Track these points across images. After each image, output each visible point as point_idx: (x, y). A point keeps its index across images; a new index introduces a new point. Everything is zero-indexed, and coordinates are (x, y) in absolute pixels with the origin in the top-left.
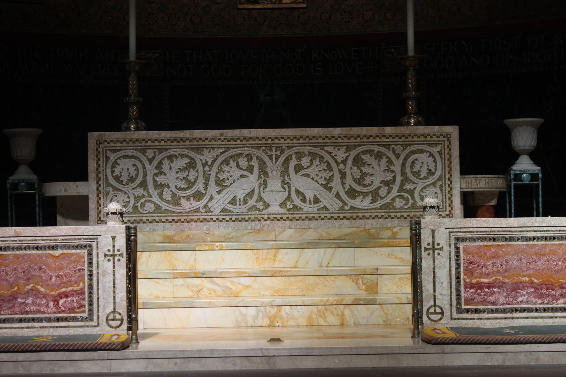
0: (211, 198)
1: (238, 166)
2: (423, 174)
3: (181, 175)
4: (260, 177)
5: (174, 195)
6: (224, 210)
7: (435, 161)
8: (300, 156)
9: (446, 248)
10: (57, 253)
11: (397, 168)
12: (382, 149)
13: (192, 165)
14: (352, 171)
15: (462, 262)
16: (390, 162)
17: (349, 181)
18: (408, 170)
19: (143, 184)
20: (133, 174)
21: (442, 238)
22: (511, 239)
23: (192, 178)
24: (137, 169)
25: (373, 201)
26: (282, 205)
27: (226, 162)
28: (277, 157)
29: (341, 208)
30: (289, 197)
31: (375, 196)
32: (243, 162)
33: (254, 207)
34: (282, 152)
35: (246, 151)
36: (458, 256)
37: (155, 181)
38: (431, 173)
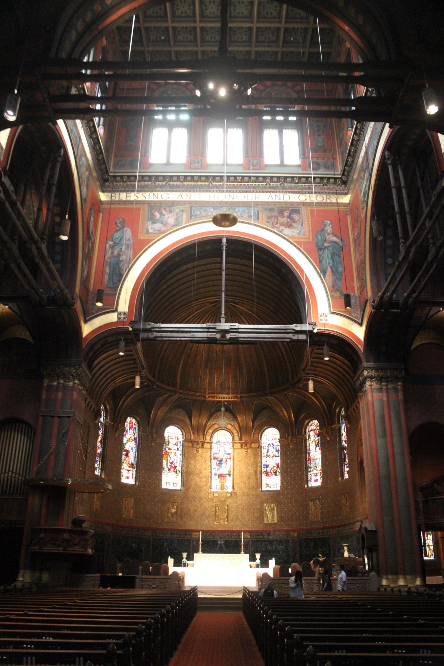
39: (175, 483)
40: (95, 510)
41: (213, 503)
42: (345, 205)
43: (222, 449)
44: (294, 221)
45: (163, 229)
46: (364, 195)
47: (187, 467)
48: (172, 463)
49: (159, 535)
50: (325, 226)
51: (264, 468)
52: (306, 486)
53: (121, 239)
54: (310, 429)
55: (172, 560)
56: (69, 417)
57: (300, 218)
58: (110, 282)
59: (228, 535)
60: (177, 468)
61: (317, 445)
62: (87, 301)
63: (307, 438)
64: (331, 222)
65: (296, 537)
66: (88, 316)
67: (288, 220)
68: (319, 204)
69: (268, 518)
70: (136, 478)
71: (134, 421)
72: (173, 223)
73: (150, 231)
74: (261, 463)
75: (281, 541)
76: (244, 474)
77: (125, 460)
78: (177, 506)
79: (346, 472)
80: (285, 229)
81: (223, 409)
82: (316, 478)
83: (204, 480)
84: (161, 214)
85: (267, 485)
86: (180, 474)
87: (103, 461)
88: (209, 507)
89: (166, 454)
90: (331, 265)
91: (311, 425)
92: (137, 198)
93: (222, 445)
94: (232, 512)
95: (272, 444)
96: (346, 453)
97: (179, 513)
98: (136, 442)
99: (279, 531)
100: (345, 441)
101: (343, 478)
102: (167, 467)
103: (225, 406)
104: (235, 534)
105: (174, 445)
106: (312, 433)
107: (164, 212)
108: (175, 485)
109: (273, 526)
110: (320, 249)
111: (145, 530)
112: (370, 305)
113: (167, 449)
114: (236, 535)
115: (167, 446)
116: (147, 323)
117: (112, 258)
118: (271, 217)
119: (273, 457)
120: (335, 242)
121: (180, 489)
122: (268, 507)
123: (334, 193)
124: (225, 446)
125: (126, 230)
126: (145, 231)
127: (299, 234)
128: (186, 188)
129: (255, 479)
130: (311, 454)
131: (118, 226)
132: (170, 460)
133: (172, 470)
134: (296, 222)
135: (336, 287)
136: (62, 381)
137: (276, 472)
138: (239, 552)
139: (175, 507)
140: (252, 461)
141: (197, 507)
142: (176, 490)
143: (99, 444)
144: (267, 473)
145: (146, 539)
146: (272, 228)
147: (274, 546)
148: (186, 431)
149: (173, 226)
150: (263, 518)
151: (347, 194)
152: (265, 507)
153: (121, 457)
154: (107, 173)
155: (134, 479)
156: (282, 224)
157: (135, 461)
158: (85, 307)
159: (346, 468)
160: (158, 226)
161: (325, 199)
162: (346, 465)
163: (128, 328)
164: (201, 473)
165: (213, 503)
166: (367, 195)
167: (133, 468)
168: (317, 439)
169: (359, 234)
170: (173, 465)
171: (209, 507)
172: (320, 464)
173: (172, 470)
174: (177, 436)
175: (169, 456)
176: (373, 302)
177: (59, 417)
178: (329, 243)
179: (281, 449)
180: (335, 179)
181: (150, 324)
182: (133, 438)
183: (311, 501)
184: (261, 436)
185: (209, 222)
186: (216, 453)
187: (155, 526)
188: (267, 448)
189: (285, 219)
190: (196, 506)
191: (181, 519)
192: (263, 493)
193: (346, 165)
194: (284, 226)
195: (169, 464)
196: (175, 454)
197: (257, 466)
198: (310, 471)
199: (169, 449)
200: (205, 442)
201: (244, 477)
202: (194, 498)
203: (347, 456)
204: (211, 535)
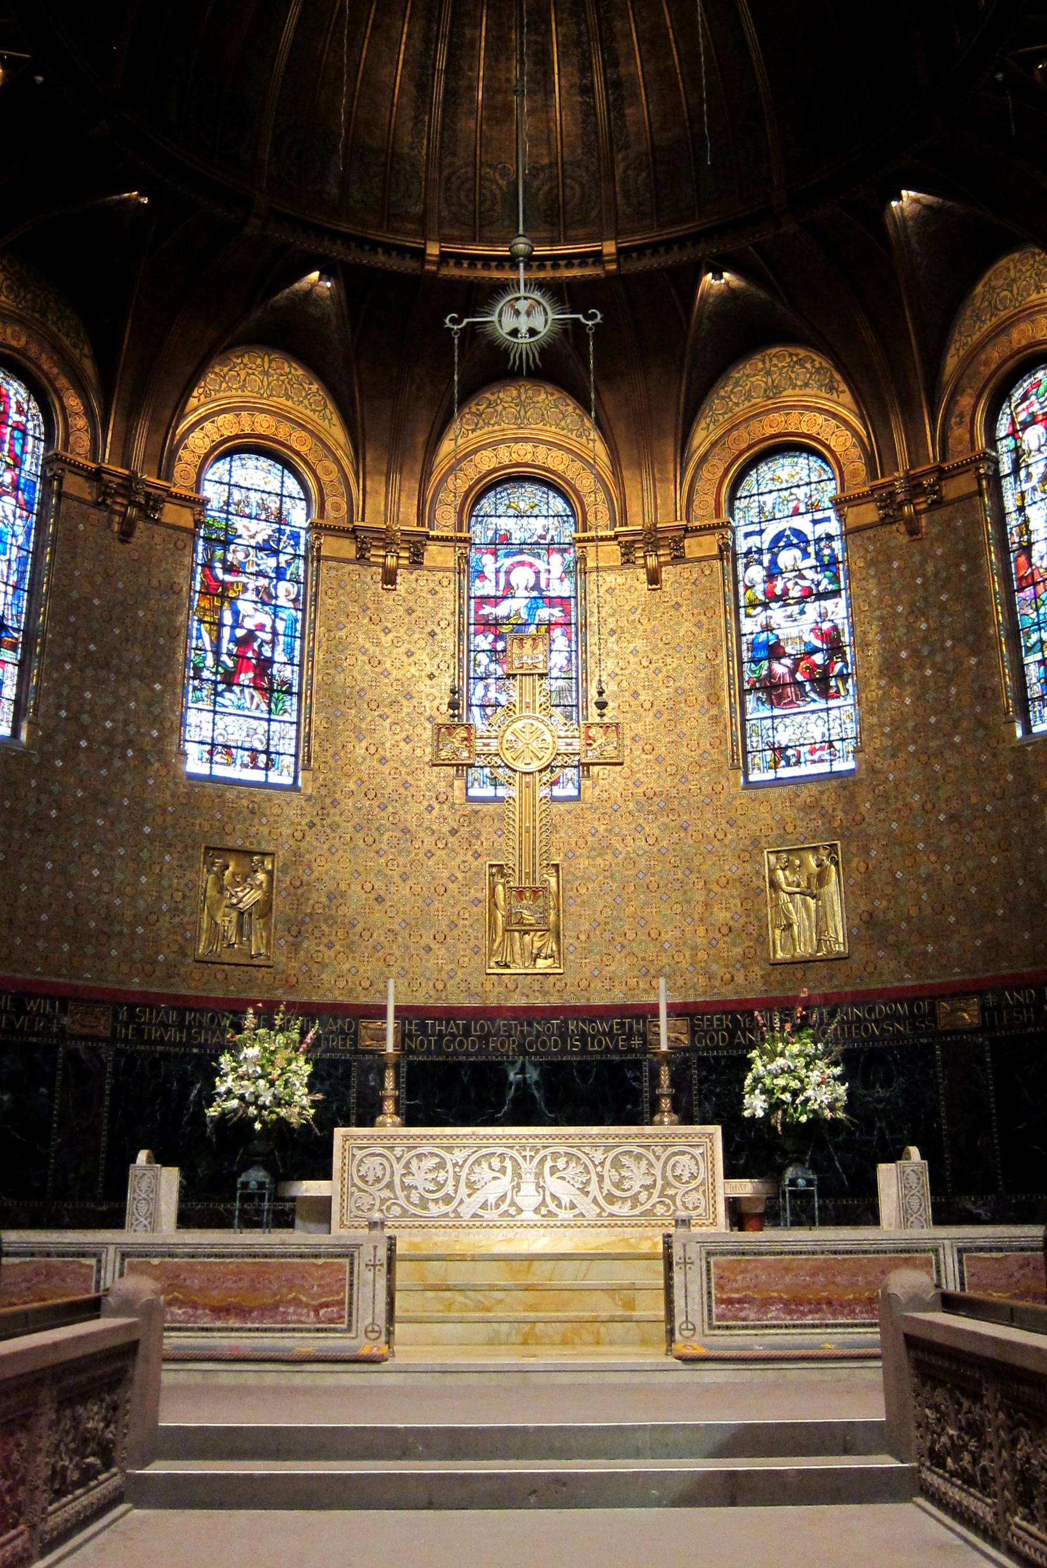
0: (462, 1202)
1: (490, 1167)
2: (685, 1178)
3: (430, 1176)
4: (513, 1180)
5: (422, 1197)
6: (475, 1215)
7: (697, 1164)
8: (555, 1156)
9: (697, 1262)
10: (320, 1261)
11: (657, 1171)
12: (641, 1150)
13: (441, 1165)
14: (610, 1174)
15: (712, 1276)
16: (651, 1165)
17: (607, 1185)
18: (669, 1174)
19: (390, 1186)
20: (380, 1174)
21: (694, 1252)
22: (761, 1254)
23: (441, 1179)
24: (384, 1169)
25: (633, 1208)
26: (537, 1210)
27: (477, 1162)
28: (532, 1157)
29: (599, 1215)
30: (543, 1203)
31: (635, 1200)
32: (496, 1163)
33: (506, 1213)
34: (537, 1151)
35: (499, 1151)
36: (708, 1270)
37: (402, 1182)
38: (693, 1177)
39: (261, 748)
41: (477, 855)
43: (522, 577)
52: (1019, 733)
54: (1022, 417)
55: (170, 1178)
63: (1006, 467)
69: (789, 926)
70: (17, 702)
74: (740, 635)
78: (270, 874)
85: (780, 751)
88: (453, 878)
89: (207, 591)
91: (1025, 397)
95: (798, 533)
97: (277, 902)
98: (27, 506)
102: (218, 662)
104: (601, 1026)
105: (259, 548)
108: (262, 759)
111: (64, 1002)
113: (218, 565)
114: (610, 1034)
115: (219, 553)
119: (801, 600)
121: (289, 781)
124: (541, 565)
132: (236, 625)
133: (245, 678)
137: (825, 679)
139: (261, 877)
142: (266, 785)
148: (324, 478)
152: (772, 871)
164: (409, 696)
165: (477, 855)
171: (453, 878)
173: (245, 678)
174: (273, 503)
175: (232, 601)
179: (845, 549)
184: (733, 498)
188: (766, 558)
191: (296, 947)
192: (752, 793)
195: (226, 645)
199: (230, 569)
200: (428, 537)
201: (649, 718)
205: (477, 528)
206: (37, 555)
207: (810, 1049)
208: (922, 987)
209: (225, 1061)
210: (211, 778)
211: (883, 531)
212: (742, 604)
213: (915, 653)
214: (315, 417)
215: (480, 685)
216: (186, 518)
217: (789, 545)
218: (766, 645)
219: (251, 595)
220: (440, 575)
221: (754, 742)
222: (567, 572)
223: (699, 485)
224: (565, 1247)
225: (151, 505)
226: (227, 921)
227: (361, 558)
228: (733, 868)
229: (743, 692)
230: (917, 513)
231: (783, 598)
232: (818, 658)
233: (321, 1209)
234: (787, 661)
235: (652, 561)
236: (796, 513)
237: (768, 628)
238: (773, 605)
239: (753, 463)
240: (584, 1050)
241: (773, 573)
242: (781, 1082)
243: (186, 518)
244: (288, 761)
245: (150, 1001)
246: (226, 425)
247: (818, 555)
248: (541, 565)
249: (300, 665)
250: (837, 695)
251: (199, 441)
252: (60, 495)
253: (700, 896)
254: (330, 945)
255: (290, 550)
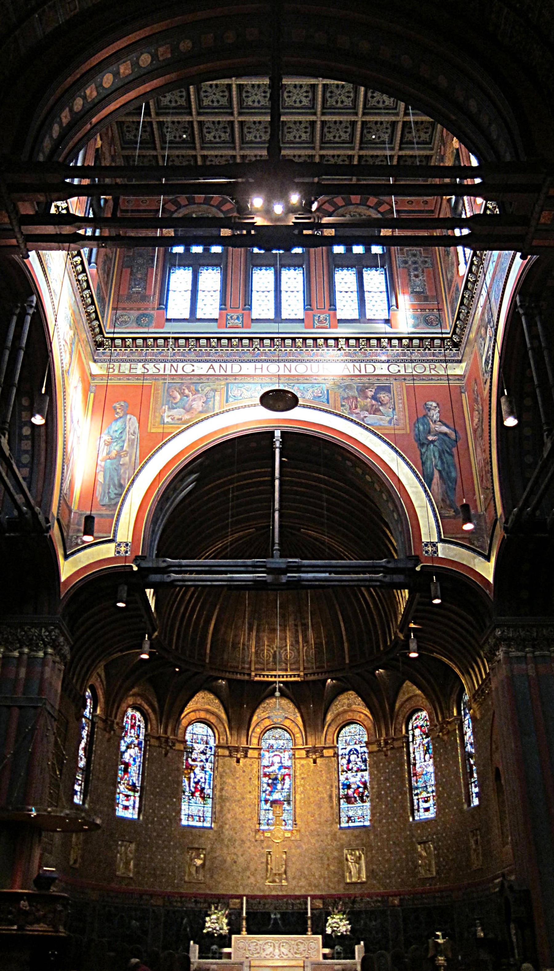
13: (257, 945)
14: (296, 947)
40: (72, 862)
41: (263, 848)
42: (459, 377)
43: (277, 759)
44: (382, 405)
45: (187, 417)
46: (487, 362)
47: (222, 789)
48: (197, 783)
49: (175, 904)
50: (429, 410)
51: (343, 789)
52: (411, 819)
53: (121, 433)
54: (415, 725)
56: (35, 708)
57: (391, 399)
58: (104, 496)
59: (287, 903)
60: (205, 791)
61: (426, 751)
62: (68, 526)
63: (411, 739)
64: (438, 404)
65: (398, 906)
66: (71, 547)
67: (374, 402)
68: (420, 377)
69: (350, 872)
71: (138, 715)
72: (200, 409)
73: (166, 420)
74: (339, 781)
75: (372, 912)
76: (312, 800)
77: (122, 779)
78: (205, 855)
79: (474, 795)
80: (369, 415)
81: (277, 694)
82: (426, 805)
83: (249, 810)
84: (182, 394)
85: (349, 818)
86: (210, 801)
87: (86, 781)
89: (187, 768)
90: (439, 468)
91: (416, 719)
92: (146, 371)
93: (276, 753)
94: (293, 863)
95: (356, 750)
96: (472, 762)
98: (140, 749)
99: (369, 895)
100: (471, 744)
101: (469, 805)
102: (190, 790)
103: (280, 689)
104: (298, 901)
106: (417, 732)
107: (187, 391)
108: (202, 818)
109: (359, 886)
110: (422, 445)
112: (501, 527)
113: (190, 760)
114: (300, 904)
116: (161, 559)
117: (108, 461)
118: (348, 398)
119: (356, 771)
120: (446, 434)
122: (351, 854)
123: (441, 361)
124: (282, 755)
125: (130, 419)
126: (158, 420)
127: (390, 422)
128: (219, 356)
129: (329, 809)
130: (418, 766)
131: (117, 413)
133: (197, 794)
134: (385, 404)
135: (448, 502)
136: (26, 650)
138: (304, 932)
139: (202, 856)
140: (324, 778)
141: (238, 856)
142: (203, 827)
143: (81, 752)
144: (349, 799)
145: (154, 911)
146: (349, 414)
147: (362, 922)
148: (220, 730)
149: (201, 412)
150: (343, 871)
151: (460, 361)
153: (116, 775)
154: (101, 332)
155: (137, 810)
156: (364, 409)
157: (138, 780)
158: (65, 534)
159: (473, 788)
160: (177, 413)
161: (428, 369)
162: (474, 782)
163: (131, 567)
164: (243, 798)
165: (263, 848)
166: (490, 362)
167: (135, 791)
168: (426, 741)
169: (481, 421)
170: (198, 787)
171: (256, 855)
172: (433, 783)
173: (197, 794)
174: (205, 738)
175: (193, 770)
176: (506, 522)
177: (20, 707)
178: (435, 435)
180: (442, 339)
181: (164, 561)
182: (136, 742)
183: (420, 843)
184: (338, 737)
185: (255, 405)
186: (268, 767)
187: (169, 889)
188: (347, 757)
189: (369, 400)
190: (235, 854)
191: (212, 877)
192: (341, 831)
193: (458, 318)
194: (367, 411)
195: (192, 784)
196: (203, 768)
197: (332, 786)
198: (417, 794)
199: (194, 760)
200: (249, 748)
201: (312, 805)
202: (232, 840)
203: (474, 768)
204: (260, 903)
205: (263, 744)
206: (144, 763)
207: (342, 917)
208: (385, 893)
209: (207, 919)
210: (189, 826)
211: (379, 754)
212: (340, 770)
213: (386, 792)
214: (216, 710)
215: (264, 794)
216: (182, 747)
217: (354, 754)
218: (346, 785)
219: (198, 768)
220: (253, 760)
221: (342, 814)
222: (290, 758)
223: (328, 733)
224: (285, 964)
225: (174, 745)
226: (193, 870)
227: (230, 756)
228: (336, 854)
229: (339, 799)
230: (387, 750)
231: (350, 770)
232: (361, 790)
233: (229, 955)
234: (352, 790)
235: (314, 757)
236: (356, 744)
237: (347, 779)
238: (349, 772)
239: (344, 726)
240: (293, 909)
241: (349, 761)
242: (334, 925)
243: (182, 747)
244: (209, 819)
245: (172, 895)
246: (193, 716)
247: (362, 758)
248: (282, 755)
249: (213, 789)
250: (365, 802)
251: (184, 722)
252: (150, 746)
253: (326, 862)
254: (221, 877)
255: (210, 753)
